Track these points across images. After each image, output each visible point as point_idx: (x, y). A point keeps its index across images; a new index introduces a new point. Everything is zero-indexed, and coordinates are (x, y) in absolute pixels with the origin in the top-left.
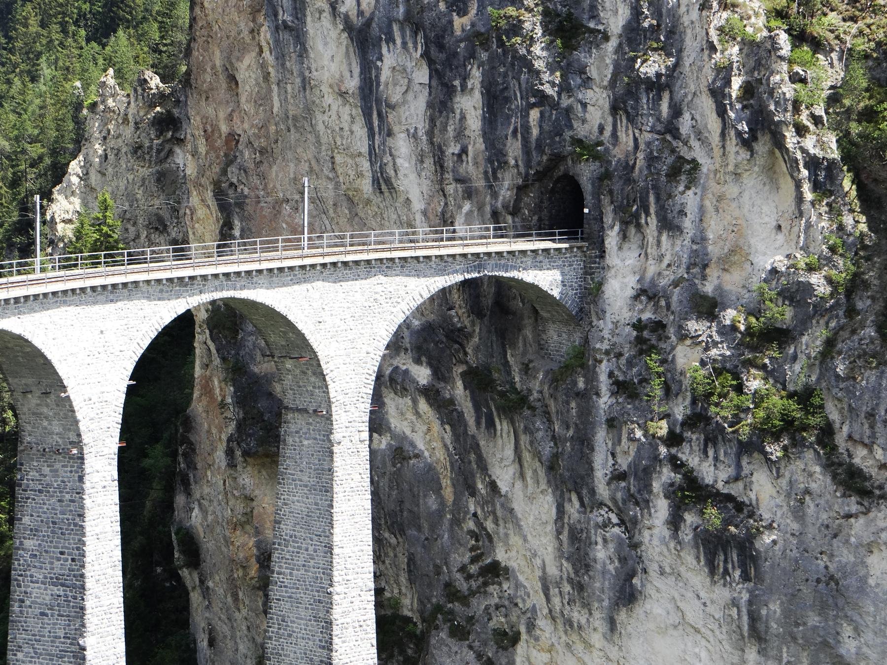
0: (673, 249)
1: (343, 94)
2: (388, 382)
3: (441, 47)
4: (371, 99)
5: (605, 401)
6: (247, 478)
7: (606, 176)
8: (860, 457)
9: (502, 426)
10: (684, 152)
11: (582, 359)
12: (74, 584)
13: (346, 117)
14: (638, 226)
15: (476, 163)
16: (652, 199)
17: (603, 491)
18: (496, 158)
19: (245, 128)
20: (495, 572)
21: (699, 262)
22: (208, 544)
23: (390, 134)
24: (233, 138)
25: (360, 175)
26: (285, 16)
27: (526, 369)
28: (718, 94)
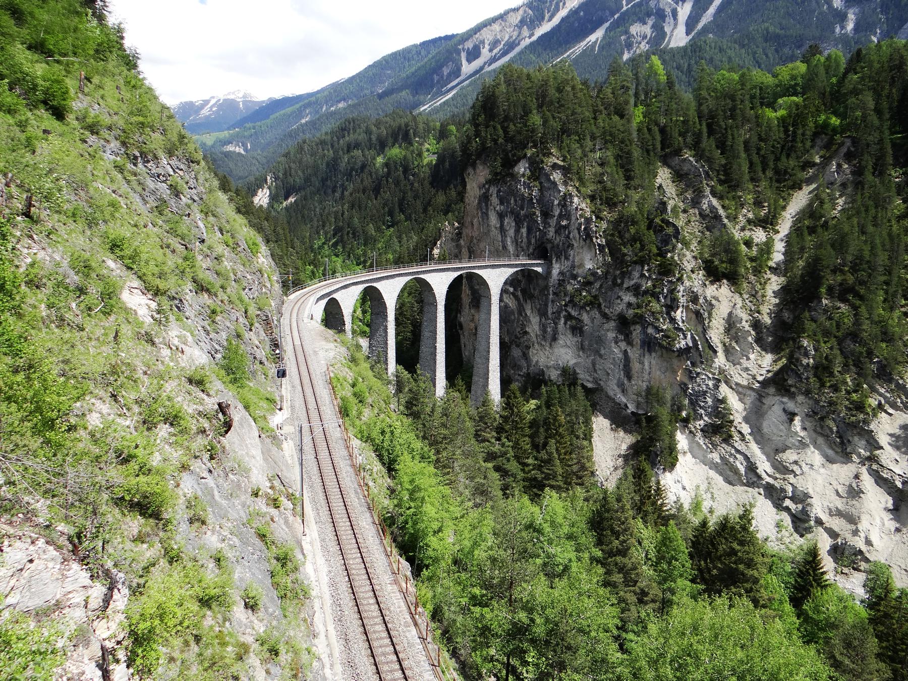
0: (568, 263)
2: (504, 291)
4: (502, 229)
5: (551, 296)
6: (472, 311)
7: (553, 247)
8: (607, 311)
9: (528, 301)
11: (547, 287)
12: (434, 333)
17: (550, 316)
18: (529, 242)
19: (475, 234)
20: (526, 333)
21: (573, 267)
22: (465, 326)
24: (472, 237)
27: (534, 289)
28: (579, 229)
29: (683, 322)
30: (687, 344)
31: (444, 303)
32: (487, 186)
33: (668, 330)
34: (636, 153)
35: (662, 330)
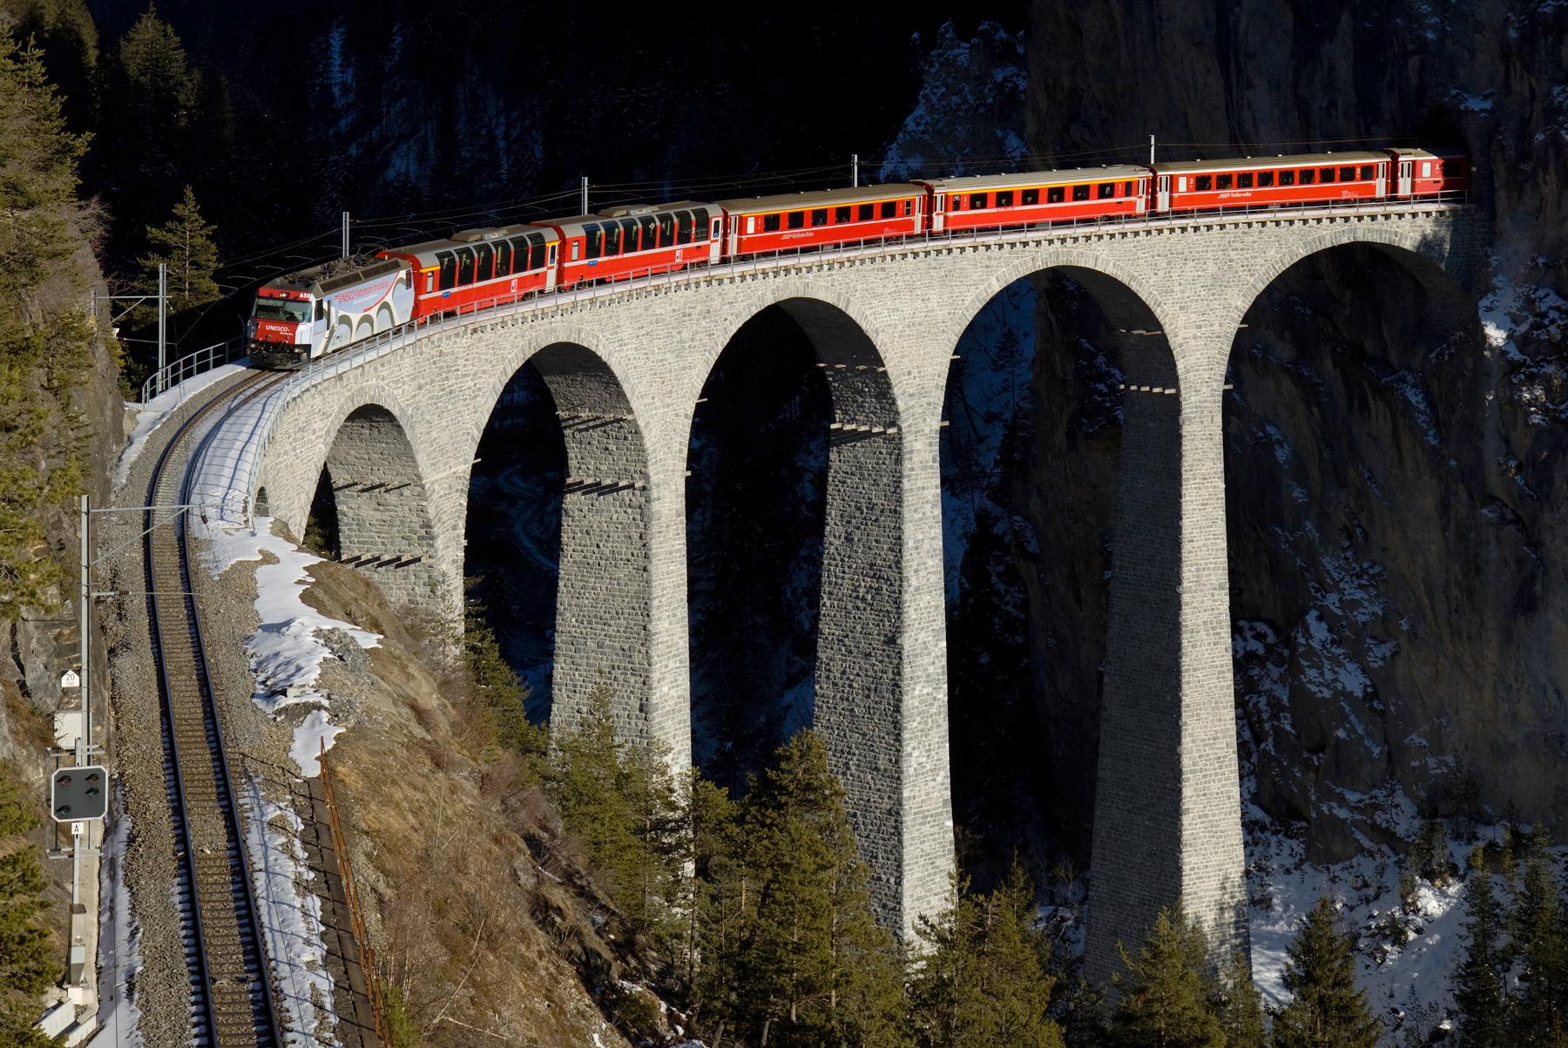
16: (1551, 153)
23: (1249, 86)
31: (935, 423)
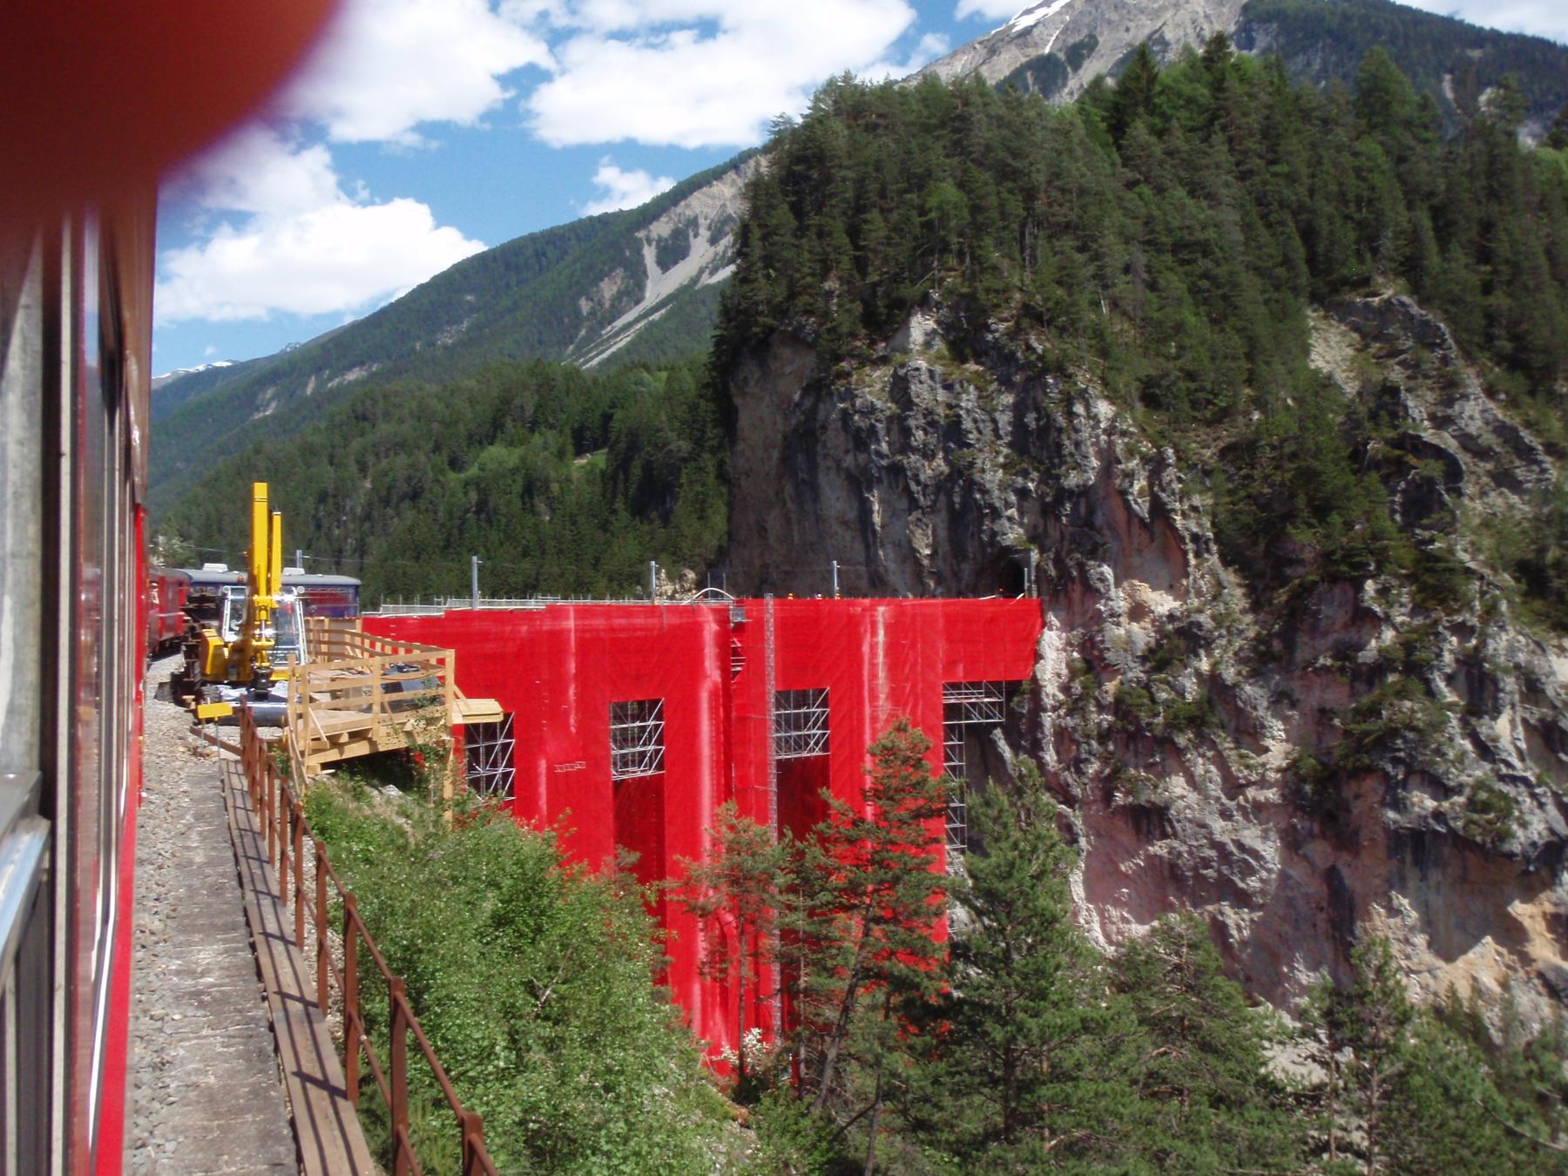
1: (846, 524)
3: (918, 483)
10: (1098, 538)
13: (848, 538)
14: (1067, 595)
15: (945, 560)
24: (765, 566)
25: (859, 577)
26: (802, 475)
29: (1522, 759)
30: (1552, 831)
32: (808, 404)
33: (1480, 785)
34: (1251, 290)
35: (1458, 790)
